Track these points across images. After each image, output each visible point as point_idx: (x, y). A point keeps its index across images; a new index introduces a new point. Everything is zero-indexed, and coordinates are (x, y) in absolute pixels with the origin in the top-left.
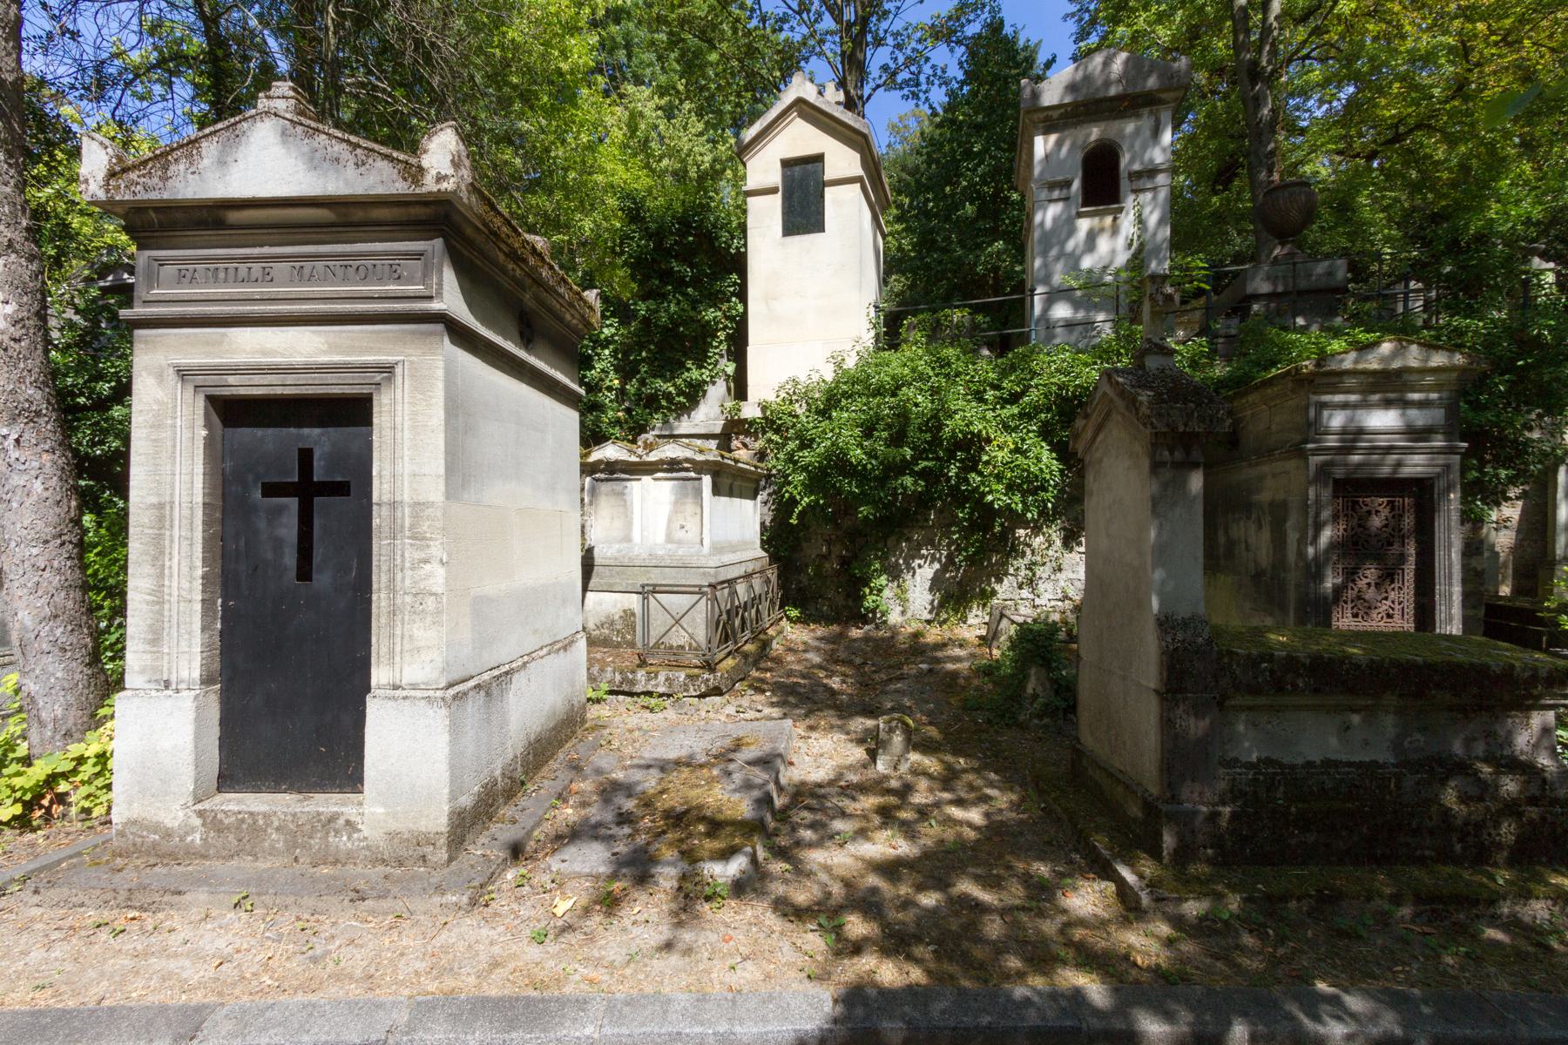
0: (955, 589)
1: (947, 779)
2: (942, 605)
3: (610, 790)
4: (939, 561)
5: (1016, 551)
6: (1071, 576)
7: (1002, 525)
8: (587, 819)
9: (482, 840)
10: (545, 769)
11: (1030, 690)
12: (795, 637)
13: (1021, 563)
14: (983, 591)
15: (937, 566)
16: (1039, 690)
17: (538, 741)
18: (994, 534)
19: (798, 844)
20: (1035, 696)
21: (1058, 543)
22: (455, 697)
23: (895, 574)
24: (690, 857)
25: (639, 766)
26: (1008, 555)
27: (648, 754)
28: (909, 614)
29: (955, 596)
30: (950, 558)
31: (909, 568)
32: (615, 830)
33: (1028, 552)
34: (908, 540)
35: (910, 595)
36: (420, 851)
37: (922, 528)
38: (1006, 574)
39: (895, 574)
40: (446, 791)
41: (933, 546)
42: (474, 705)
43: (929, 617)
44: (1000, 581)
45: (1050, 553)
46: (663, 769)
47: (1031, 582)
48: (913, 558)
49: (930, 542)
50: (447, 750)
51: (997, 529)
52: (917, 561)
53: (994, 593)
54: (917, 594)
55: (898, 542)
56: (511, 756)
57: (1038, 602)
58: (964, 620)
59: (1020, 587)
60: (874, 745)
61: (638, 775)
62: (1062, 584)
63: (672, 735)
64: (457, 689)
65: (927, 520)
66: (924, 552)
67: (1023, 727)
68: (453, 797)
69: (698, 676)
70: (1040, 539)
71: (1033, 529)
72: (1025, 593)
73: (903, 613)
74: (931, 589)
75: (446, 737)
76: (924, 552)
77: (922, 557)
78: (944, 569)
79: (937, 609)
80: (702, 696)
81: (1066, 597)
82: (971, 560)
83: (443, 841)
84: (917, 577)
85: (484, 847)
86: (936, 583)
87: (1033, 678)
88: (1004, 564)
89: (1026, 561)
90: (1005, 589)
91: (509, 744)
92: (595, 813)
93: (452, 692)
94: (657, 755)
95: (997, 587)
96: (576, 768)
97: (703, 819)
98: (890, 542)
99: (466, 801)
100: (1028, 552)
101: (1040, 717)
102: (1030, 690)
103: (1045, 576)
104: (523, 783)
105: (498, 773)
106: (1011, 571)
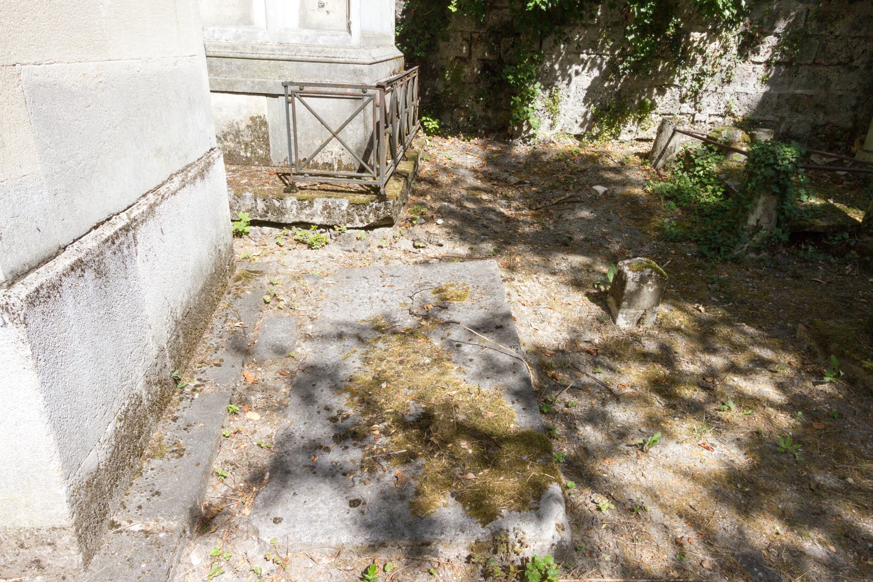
0: (612, 101)
1: (704, 337)
2: (595, 118)
3: (309, 382)
4: (600, 68)
5: (686, 58)
6: (739, 89)
7: (676, 26)
8: (288, 437)
9: (137, 498)
10: (200, 348)
11: (752, 221)
12: (458, 155)
13: (689, 72)
14: (642, 105)
15: (596, 73)
16: (764, 221)
17: (187, 315)
18: (666, 37)
19: (587, 451)
20: (757, 228)
21: (734, 50)
22: (32, 301)
23: (549, 84)
24: (479, 507)
25: (325, 337)
26: (677, 63)
27: (335, 314)
28: (558, 128)
29: (612, 107)
30: (613, 66)
31: (565, 75)
32: (334, 456)
33: (700, 60)
34: (568, 41)
35: (562, 107)
36: (28, 555)
37: (585, 26)
38: (671, 85)
39: (549, 84)
40: (56, 464)
41: (595, 49)
42: (76, 306)
43: (579, 131)
44: (662, 92)
45: (723, 61)
46: (360, 339)
47: (695, 96)
48: (571, 63)
49: (593, 45)
50: (38, 401)
51: (671, 31)
52: (575, 67)
53: (653, 106)
54: (570, 106)
55: (556, 43)
56: (155, 352)
57: (698, 117)
58: (615, 136)
59: (682, 101)
60: (610, 298)
61: (332, 353)
62: (727, 97)
63: (356, 281)
64: (34, 280)
65: (593, 17)
66: (584, 56)
67: (736, 261)
68: (70, 465)
69: (365, 205)
70: (717, 44)
71: (710, 33)
72: (687, 107)
73: (552, 126)
74: (585, 101)
75: (32, 379)
76: (584, 56)
77: (583, 62)
78: (604, 77)
79: (592, 121)
80: (370, 228)
81: (729, 113)
82: (636, 68)
83: (68, 538)
84: (573, 85)
85: (144, 516)
86: (592, 94)
87: (759, 210)
88: (670, 73)
89: (695, 70)
90: (666, 102)
91: (150, 333)
92: (303, 425)
93: (22, 290)
94: (342, 316)
95: (658, 99)
96: (242, 349)
97: (464, 430)
98: (547, 43)
99: (96, 457)
100: (700, 60)
101: (758, 250)
102: (752, 221)
103: (712, 88)
104: (177, 381)
105: (140, 387)
106: (677, 82)
